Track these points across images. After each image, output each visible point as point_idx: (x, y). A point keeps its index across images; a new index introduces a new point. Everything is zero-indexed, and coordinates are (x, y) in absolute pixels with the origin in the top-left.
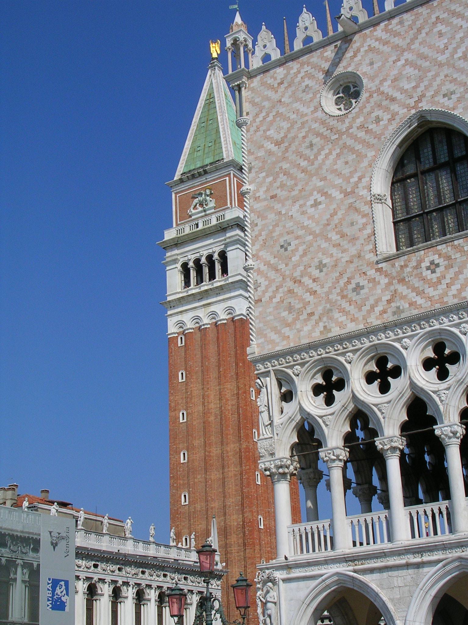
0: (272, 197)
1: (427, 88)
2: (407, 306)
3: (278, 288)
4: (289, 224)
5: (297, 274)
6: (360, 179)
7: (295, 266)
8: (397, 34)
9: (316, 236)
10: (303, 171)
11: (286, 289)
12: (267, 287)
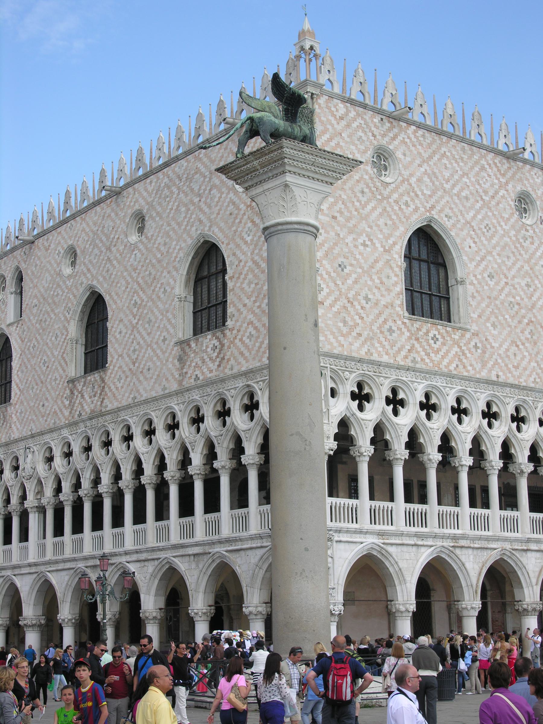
0: (334, 218)
1: (437, 202)
2: (419, 360)
3: (336, 300)
4: (346, 250)
5: (350, 295)
6: (395, 244)
7: (350, 289)
8: (421, 144)
9: (364, 272)
10: (356, 210)
11: (342, 304)
12: (329, 294)
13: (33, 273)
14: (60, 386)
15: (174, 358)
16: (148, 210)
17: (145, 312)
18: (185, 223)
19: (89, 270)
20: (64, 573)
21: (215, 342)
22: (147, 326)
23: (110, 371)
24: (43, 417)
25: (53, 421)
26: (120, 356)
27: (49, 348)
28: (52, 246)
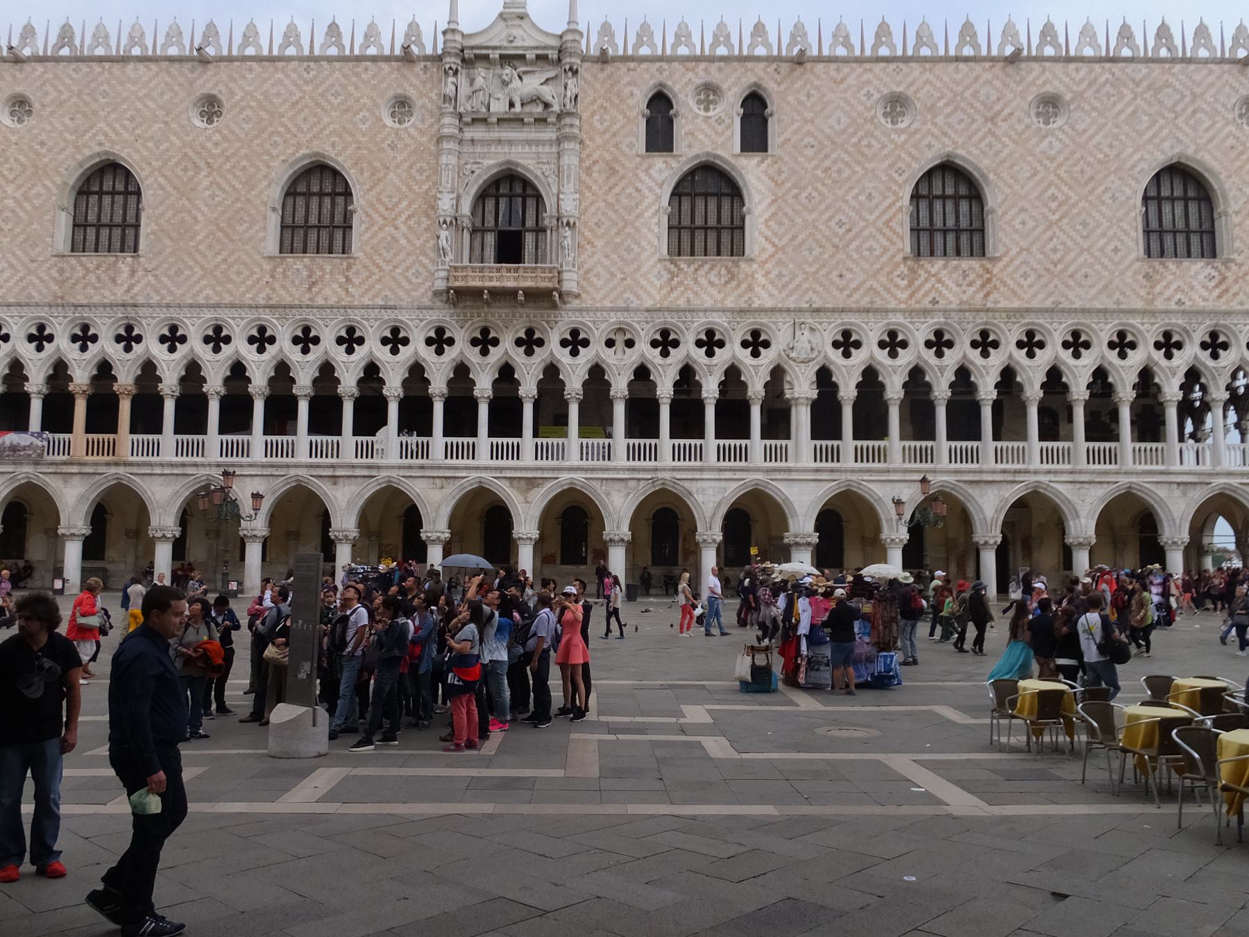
13: (800, 103)
14: (884, 259)
15: (1137, 272)
16: (1072, 100)
17: (1075, 211)
18: (1151, 133)
19: (945, 134)
20: (903, 485)
21: (1209, 270)
22: (1079, 227)
23: (1001, 264)
24: (841, 290)
25: (867, 299)
26: (1027, 250)
27: (854, 209)
28: (851, 80)
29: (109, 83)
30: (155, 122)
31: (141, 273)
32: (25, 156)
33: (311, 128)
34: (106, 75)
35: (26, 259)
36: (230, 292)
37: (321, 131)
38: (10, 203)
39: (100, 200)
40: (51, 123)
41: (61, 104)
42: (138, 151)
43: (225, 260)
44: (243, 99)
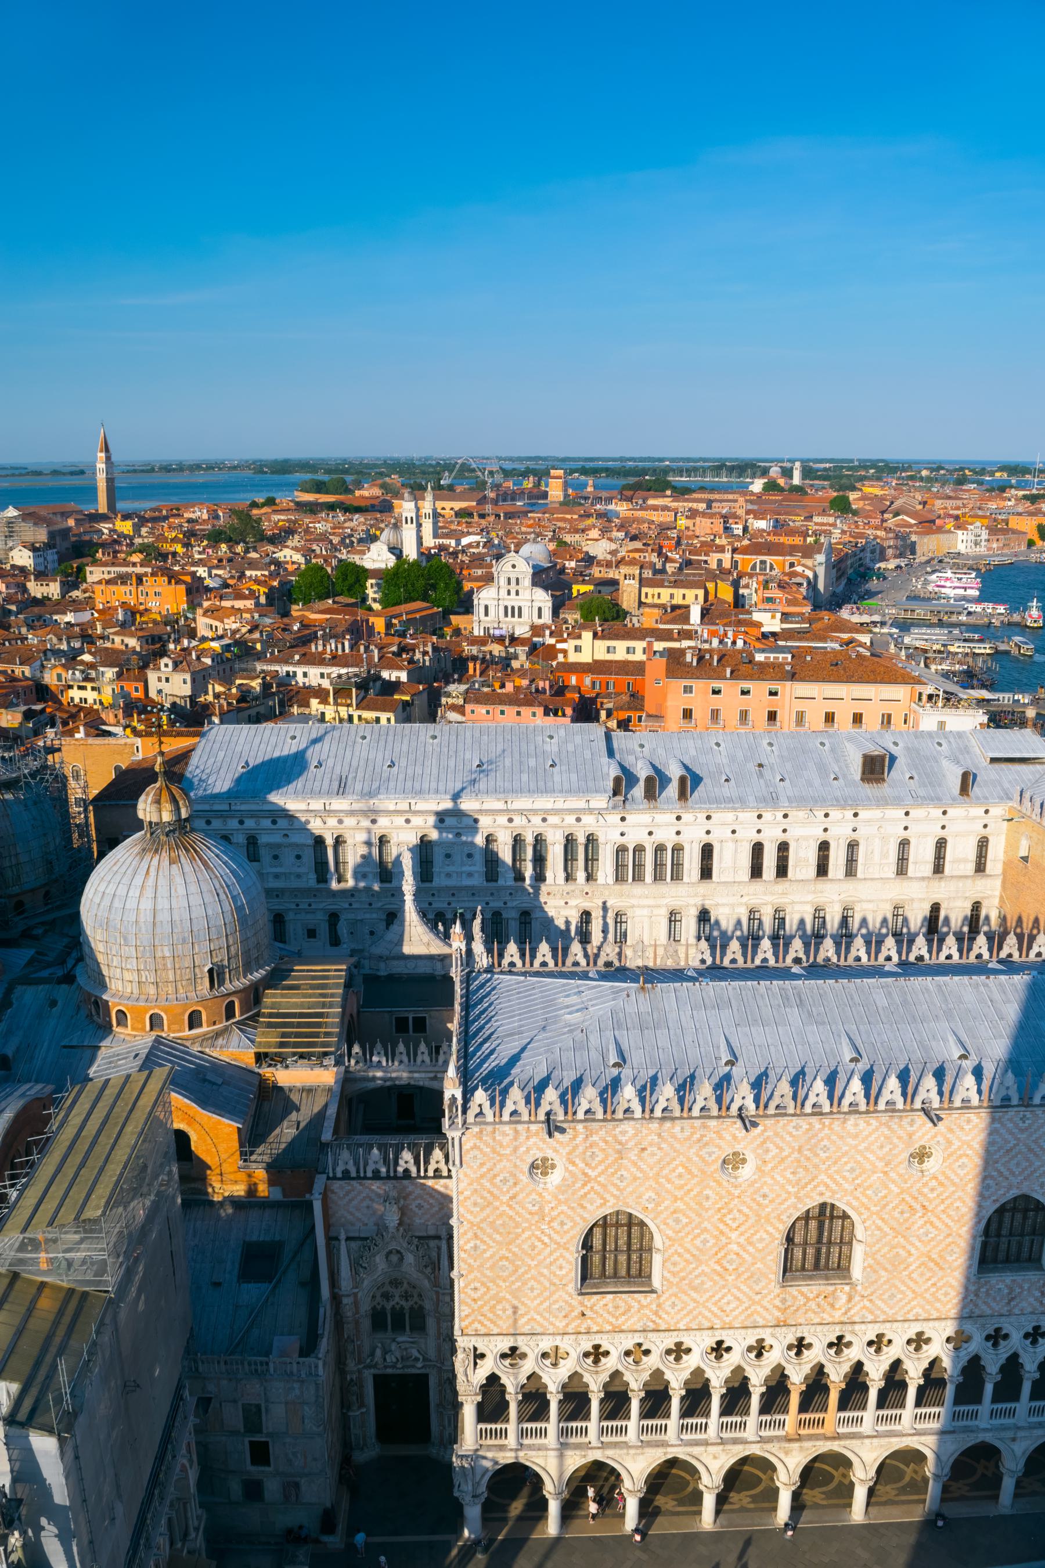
29: (829, 1138)
30: (874, 1172)
31: (857, 1298)
32: (749, 1207)
33: (1023, 1171)
34: (826, 1131)
35: (751, 1294)
36: (937, 1310)
37: (1032, 1173)
38: (734, 1247)
39: (807, 1224)
40: (773, 1178)
41: (783, 1160)
42: (857, 1198)
43: (934, 1284)
44: (959, 1148)
